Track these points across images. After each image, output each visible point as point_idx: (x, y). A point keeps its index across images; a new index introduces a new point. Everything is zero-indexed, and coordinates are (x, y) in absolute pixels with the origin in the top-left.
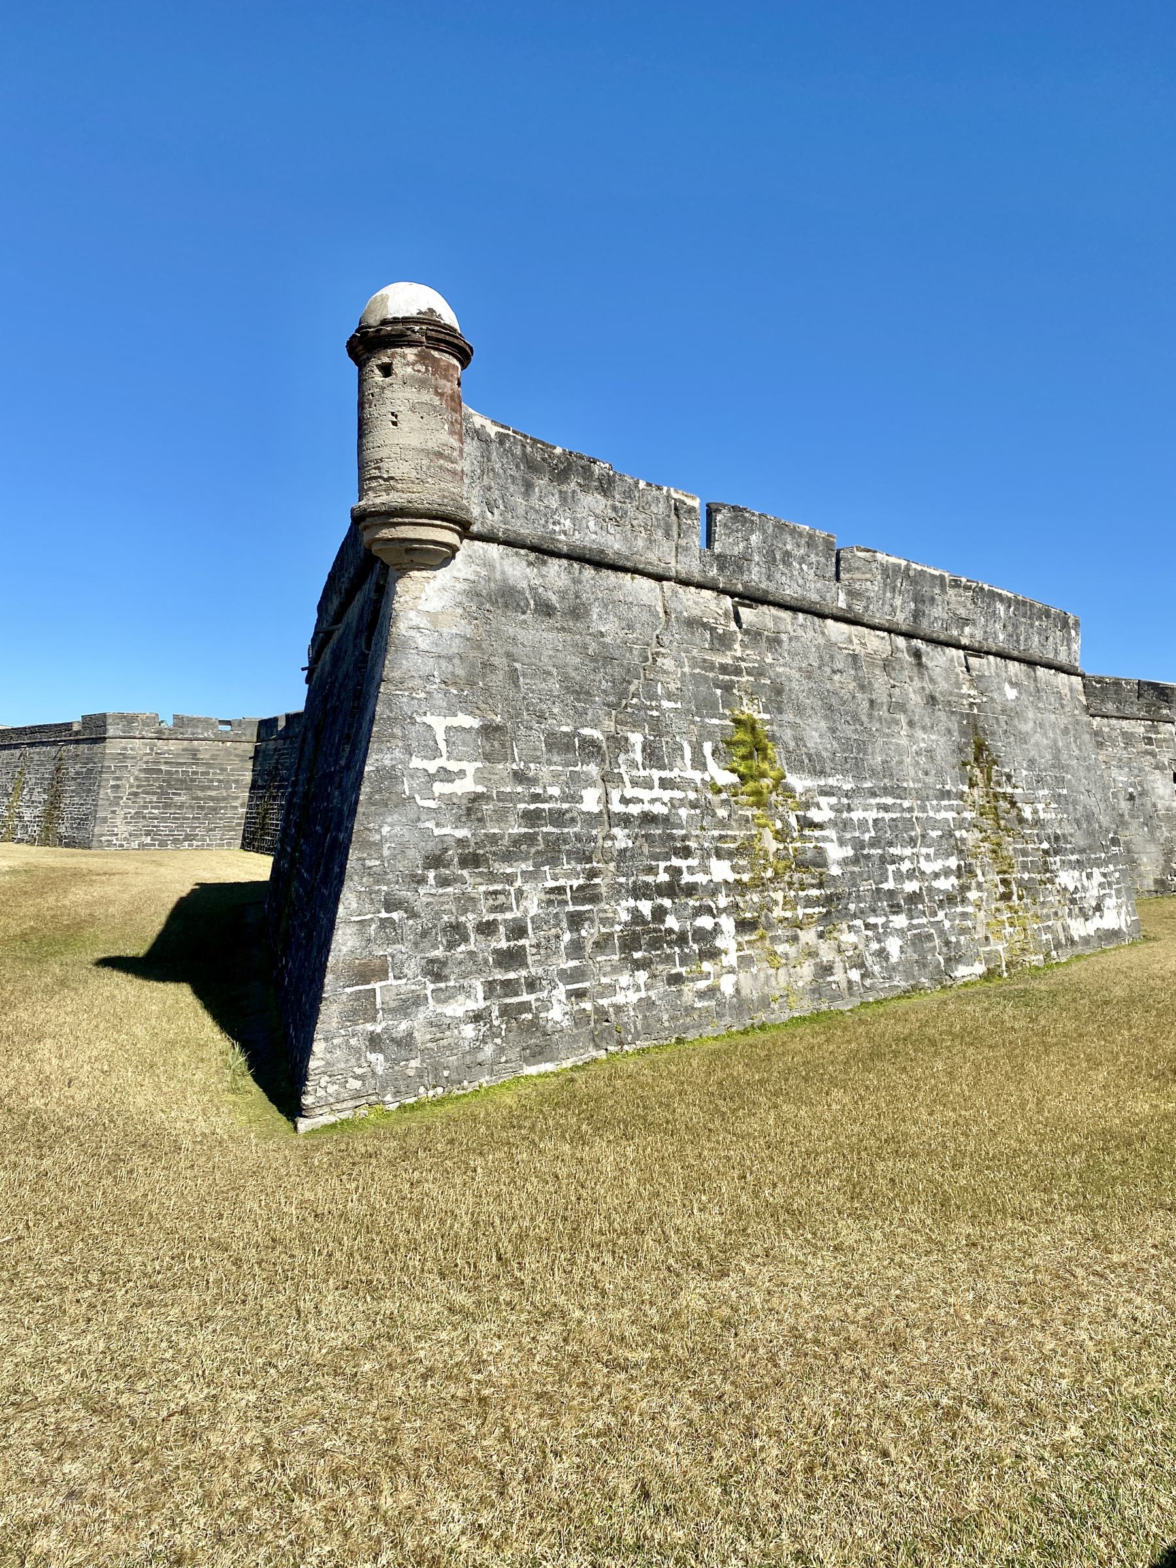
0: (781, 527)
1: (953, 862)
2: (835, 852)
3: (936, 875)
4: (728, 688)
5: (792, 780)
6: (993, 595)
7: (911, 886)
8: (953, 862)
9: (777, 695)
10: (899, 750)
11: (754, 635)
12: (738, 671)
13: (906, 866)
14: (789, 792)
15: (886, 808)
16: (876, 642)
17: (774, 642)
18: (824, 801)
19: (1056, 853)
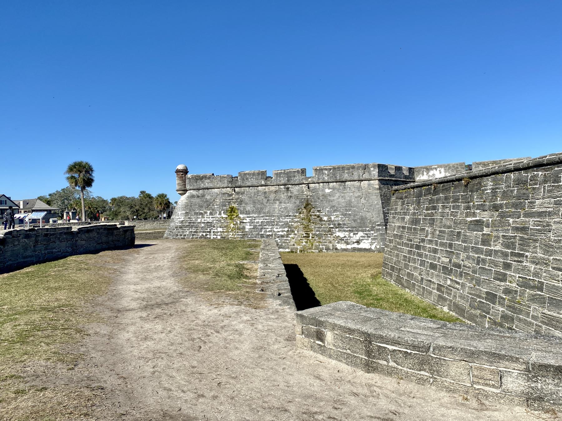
0: (245, 174)
1: (286, 229)
2: (248, 227)
3: (279, 232)
4: (230, 202)
5: (240, 215)
6: (322, 169)
7: (268, 233)
8: (286, 229)
9: (241, 202)
10: (274, 208)
11: (238, 193)
12: (233, 199)
13: (268, 230)
14: (240, 218)
15: (266, 219)
16: (273, 188)
17: (243, 193)
18: (248, 219)
19: (336, 228)
